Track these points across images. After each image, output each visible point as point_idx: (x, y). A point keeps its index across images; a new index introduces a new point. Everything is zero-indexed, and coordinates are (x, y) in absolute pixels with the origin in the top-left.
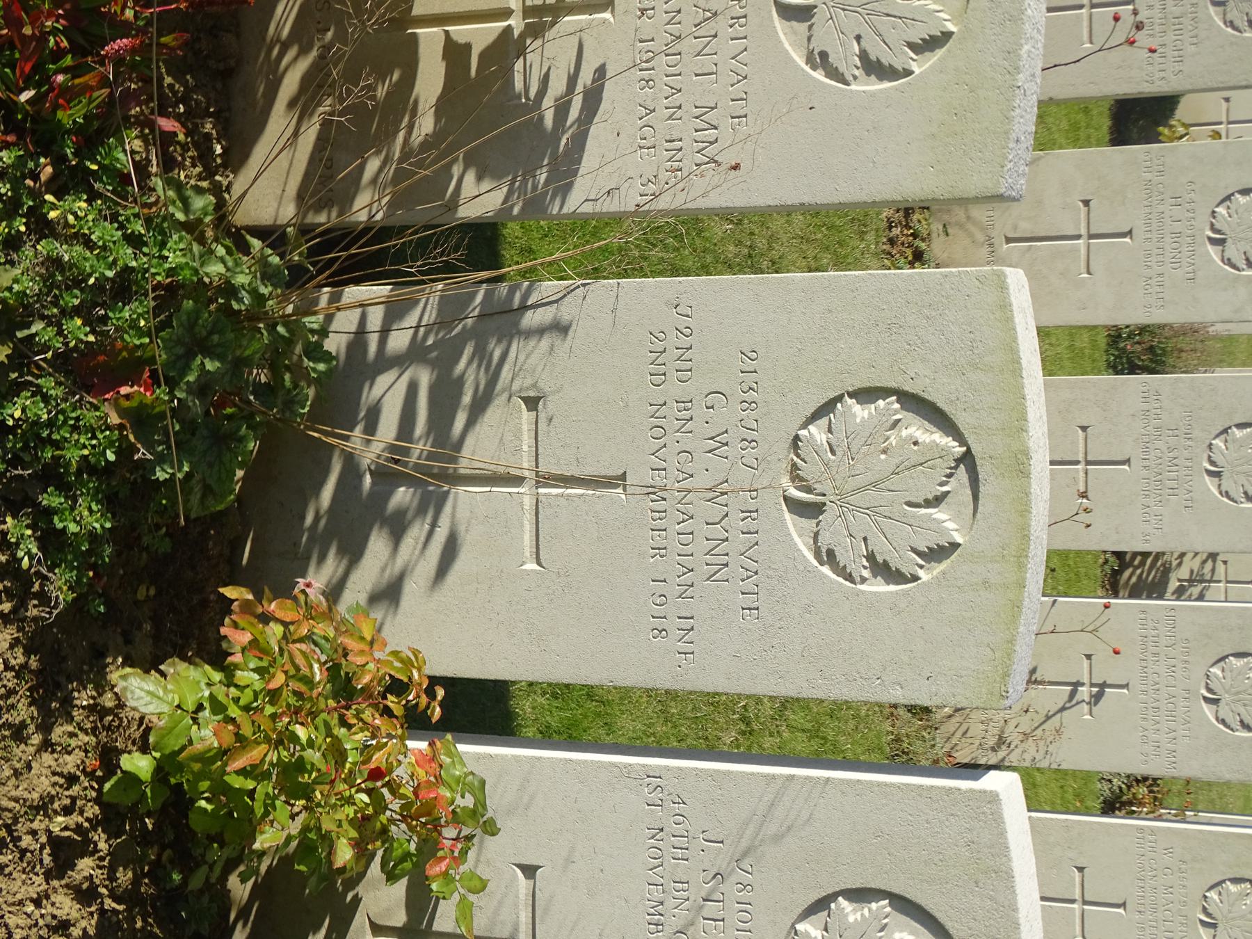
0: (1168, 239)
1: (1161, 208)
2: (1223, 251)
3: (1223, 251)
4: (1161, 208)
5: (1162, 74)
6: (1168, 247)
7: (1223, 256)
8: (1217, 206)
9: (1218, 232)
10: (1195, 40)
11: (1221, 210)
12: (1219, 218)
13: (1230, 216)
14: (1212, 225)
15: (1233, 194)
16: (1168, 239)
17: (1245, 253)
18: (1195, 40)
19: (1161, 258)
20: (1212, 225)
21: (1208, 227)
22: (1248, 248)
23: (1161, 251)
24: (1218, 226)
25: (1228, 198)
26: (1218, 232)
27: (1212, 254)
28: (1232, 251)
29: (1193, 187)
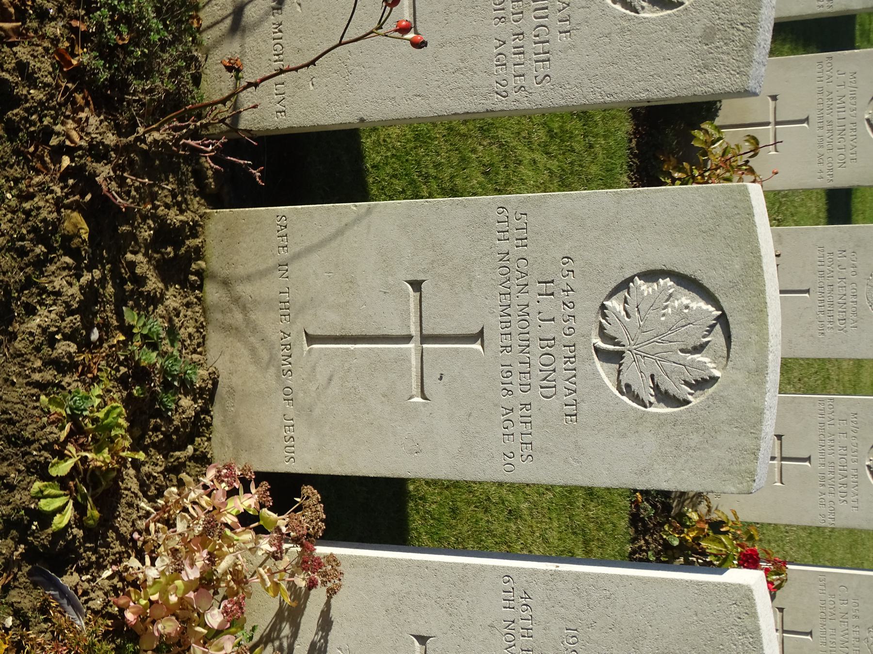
0: (536, 349)
1: (524, 298)
2: (619, 372)
3: (619, 372)
4: (524, 298)
5: (520, 81)
6: (535, 361)
7: (619, 381)
8: (609, 297)
9: (612, 340)
10: (567, 26)
11: (615, 305)
12: (611, 317)
13: (628, 316)
14: (602, 328)
15: (631, 279)
16: (536, 349)
17: (652, 377)
18: (567, 26)
19: (525, 379)
20: (602, 328)
21: (595, 332)
22: (657, 370)
23: (525, 368)
24: (610, 330)
25: (625, 285)
26: (612, 340)
27: (603, 375)
28: (632, 374)
29: (571, 265)
